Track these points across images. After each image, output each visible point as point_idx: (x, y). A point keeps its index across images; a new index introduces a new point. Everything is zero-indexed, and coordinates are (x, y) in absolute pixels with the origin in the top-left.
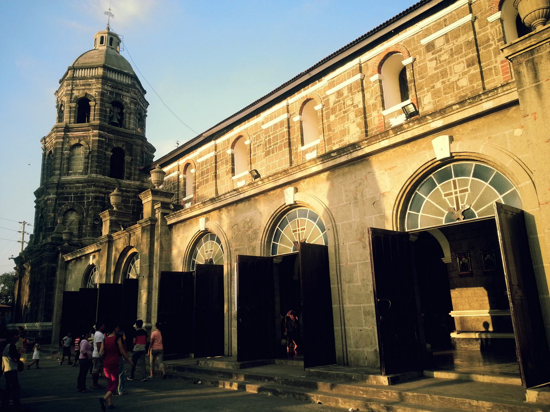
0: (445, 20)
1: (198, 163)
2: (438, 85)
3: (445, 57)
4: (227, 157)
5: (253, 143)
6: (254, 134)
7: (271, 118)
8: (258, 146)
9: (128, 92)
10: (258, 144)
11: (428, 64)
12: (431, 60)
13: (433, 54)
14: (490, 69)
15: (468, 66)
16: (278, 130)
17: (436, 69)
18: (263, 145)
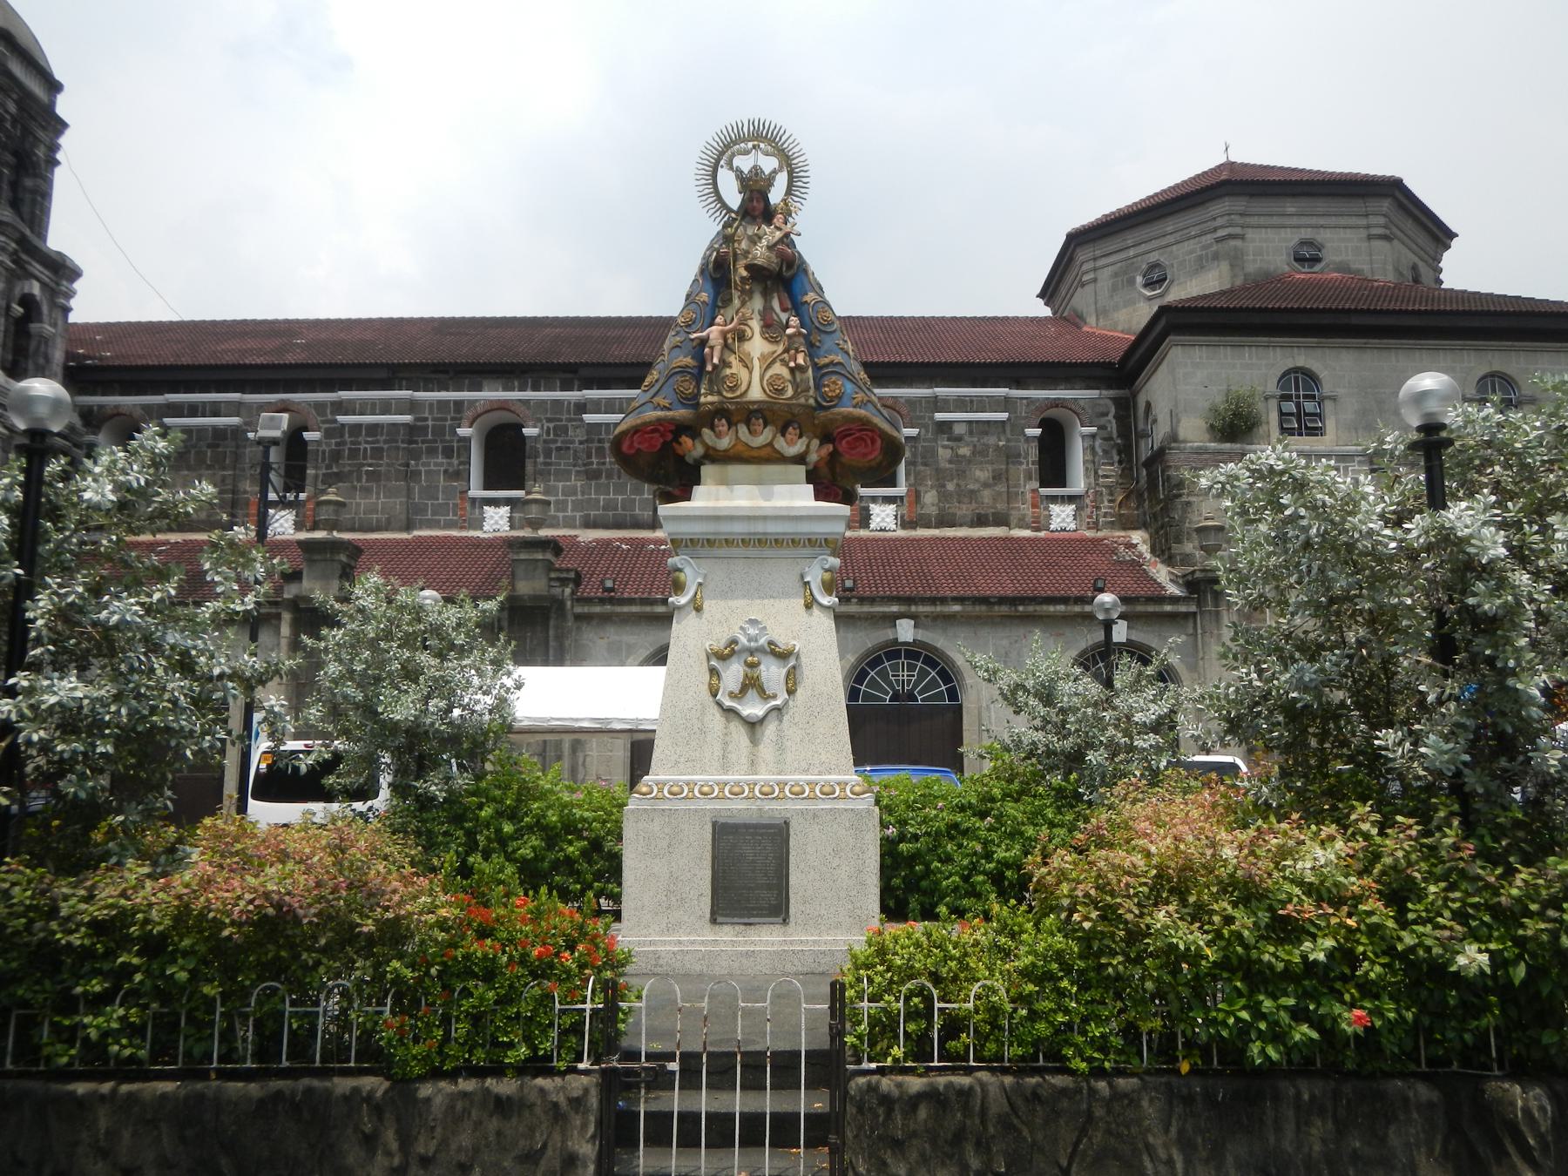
0: (972, 402)
1: (335, 421)
2: (950, 487)
3: (965, 451)
4: (452, 441)
6: (549, 420)
8: (559, 449)
9: (44, 128)
11: (940, 450)
12: (945, 447)
13: (949, 440)
14: (1017, 494)
15: (994, 478)
17: (950, 462)
18: (575, 451)
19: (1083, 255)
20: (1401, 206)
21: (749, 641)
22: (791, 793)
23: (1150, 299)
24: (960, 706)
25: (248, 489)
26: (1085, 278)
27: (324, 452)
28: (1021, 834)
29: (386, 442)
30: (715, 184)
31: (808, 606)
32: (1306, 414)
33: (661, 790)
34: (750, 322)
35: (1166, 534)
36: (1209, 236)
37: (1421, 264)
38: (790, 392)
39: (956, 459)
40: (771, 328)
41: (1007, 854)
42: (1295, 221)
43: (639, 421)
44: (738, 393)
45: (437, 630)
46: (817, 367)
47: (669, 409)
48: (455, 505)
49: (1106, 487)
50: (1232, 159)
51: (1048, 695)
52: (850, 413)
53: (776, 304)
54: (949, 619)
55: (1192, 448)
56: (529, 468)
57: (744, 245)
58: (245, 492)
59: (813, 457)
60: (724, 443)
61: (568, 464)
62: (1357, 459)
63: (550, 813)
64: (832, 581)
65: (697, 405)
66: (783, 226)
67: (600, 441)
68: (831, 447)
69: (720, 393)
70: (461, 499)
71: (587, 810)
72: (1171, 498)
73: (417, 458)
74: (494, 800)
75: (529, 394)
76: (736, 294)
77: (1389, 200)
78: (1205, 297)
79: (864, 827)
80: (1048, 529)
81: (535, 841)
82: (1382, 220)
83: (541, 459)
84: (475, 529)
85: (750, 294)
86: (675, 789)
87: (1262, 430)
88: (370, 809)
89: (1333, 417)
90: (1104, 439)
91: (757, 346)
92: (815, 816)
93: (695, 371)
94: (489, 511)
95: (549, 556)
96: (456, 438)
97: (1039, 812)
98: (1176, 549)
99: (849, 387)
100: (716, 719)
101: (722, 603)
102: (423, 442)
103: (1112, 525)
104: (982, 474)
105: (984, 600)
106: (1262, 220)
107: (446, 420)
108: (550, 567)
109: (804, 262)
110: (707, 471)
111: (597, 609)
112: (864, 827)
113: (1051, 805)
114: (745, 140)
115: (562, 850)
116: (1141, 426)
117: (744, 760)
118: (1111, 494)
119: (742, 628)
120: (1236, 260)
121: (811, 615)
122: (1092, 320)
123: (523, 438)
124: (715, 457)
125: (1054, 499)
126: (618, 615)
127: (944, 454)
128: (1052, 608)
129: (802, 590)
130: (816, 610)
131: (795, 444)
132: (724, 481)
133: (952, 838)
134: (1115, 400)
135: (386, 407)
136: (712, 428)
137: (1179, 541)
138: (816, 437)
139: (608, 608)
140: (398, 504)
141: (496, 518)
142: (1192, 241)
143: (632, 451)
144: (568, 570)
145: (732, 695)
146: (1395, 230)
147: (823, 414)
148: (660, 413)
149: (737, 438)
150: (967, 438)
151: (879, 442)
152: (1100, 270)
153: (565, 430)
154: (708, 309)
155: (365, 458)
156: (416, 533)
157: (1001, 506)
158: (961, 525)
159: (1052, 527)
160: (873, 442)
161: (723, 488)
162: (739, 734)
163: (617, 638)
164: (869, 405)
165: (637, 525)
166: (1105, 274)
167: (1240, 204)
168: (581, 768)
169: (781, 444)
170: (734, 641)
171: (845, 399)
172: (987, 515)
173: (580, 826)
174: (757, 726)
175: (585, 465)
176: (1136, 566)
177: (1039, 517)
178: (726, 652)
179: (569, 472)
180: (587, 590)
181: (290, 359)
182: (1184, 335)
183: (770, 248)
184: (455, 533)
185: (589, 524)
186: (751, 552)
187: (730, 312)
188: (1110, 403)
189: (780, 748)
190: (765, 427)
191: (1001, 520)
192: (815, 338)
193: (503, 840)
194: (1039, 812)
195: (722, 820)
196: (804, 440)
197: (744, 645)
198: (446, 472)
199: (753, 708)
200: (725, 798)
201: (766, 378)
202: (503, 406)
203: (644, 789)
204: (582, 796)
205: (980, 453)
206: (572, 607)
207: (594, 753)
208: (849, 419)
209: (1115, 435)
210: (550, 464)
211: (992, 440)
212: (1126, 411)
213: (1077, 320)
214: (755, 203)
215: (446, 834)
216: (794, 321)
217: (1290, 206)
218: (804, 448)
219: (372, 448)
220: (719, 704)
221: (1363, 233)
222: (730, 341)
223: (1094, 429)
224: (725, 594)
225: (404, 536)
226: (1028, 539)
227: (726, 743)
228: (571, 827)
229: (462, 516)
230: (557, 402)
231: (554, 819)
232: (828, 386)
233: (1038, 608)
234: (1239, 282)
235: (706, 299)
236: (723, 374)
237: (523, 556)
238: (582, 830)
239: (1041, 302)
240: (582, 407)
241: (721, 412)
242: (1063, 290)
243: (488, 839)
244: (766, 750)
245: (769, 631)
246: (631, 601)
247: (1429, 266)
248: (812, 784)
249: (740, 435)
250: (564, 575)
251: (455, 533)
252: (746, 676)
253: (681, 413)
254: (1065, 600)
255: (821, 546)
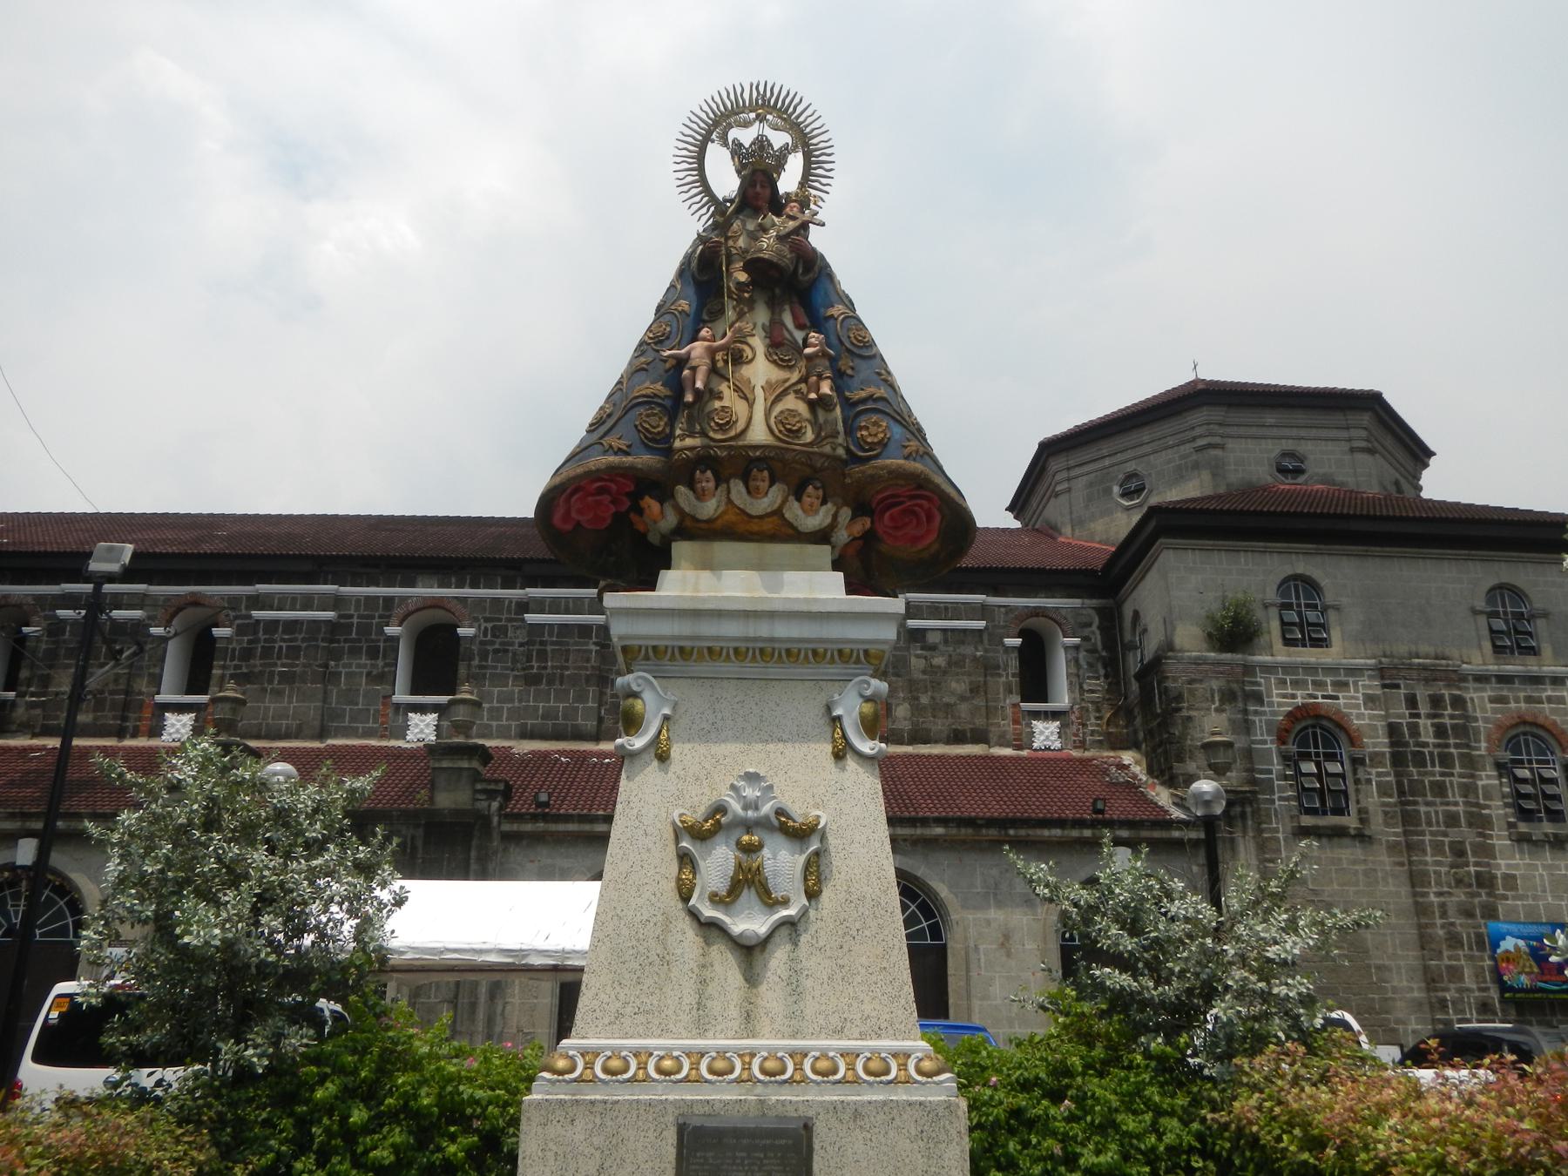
1: (250, 617)
2: (924, 700)
3: (939, 661)
5: (482, 638)
6: (487, 620)
7: (555, 606)
8: (496, 651)
10: (497, 646)
11: (913, 660)
12: (918, 656)
13: (922, 649)
15: (971, 691)
16: (571, 641)
17: (924, 672)
18: (514, 654)
19: (1055, 464)
20: (1382, 422)
21: (746, 808)
22: (815, 1072)
23: (1128, 509)
24: (944, 947)
25: (144, 689)
26: (1058, 488)
27: (234, 650)
28: (1115, 1126)
29: (303, 640)
30: (701, 169)
31: (839, 756)
32: (1309, 624)
33: (589, 1066)
34: (751, 340)
35: (1166, 752)
36: (1188, 445)
37: (1402, 481)
38: (809, 436)
39: (930, 670)
40: (779, 348)
41: (1102, 1159)
42: (1275, 432)
43: (579, 470)
44: (732, 433)
45: (282, 817)
46: (848, 404)
47: (627, 454)
48: (377, 711)
49: (1092, 702)
50: (1201, 377)
51: (1134, 921)
52: (900, 466)
53: (788, 319)
54: (930, 843)
55: (1189, 658)
56: (462, 671)
57: (741, 243)
58: (140, 693)
59: (842, 536)
60: (709, 508)
61: (507, 668)
62: (1366, 673)
63: (424, 1091)
64: (876, 716)
65: (669, 452)
66: (799, 215)
67: (542, 643)
68: (867, 522)
69: (704, 434)
70: (384, 704)
71: (481, 1087)
72: (1170, 712)
73: (338, 658)
74: (341, 1070)
75: (467, 592)
76: (730, 305)
77: (1370, 413)
78: (1194, 500)
79: (943, 1137)
80: (1030, 747)
81: (398, 1136)
82: (1364, 434)
83: (476, 662)
84: (397, 738)
85: (751, 304)
86: (615, 1064)
87: (1263, 640)
88: (159, 1083)
89: (1338, 628)
90: (1087, 651)
91: (760, 371)
92: (857, 1113)
93: (668, 403)
94: (414, 718)
95: (475, 764)
96: (382, 638)
97: (1138, 1091)
98: (1178, 768)
99: (897, 431)
100: (687, 939)
101: (702, 749)
102: (346, 641)
103: (1099, 744)
104: (958, 685)
105: (970, 822)
106: (1242, 431)
107: (373, 617)
108: (476, 777)
109: (828, 266)
110: (680, 549)
111: (528, 827)
112: (943, 1137)
113: (1151, 1084)
114: (743, 109)
115: (439, 1149)
116: (1128, 637)
117: (734, 1012)
118: (1098, 710)
119: (733, 787)
120: (1217, 470)
121: (843, 769)
122: (1067, 530)
123: (458, 638)
124: (692, 529)
125: (1037, 715)
126: (552, 834)
127: (917, 664)
128: (1046, 833)
129: (828, 729)
130: (851, 763)
131: (816, 512)
132: (707, 565)
133: (1012, 1132)
134: (1098, 610)
135: (307, 602)
136: (691, 485)
137: (1181, 760)
138: (848, 505)
139: (541, 826)
140: (312, 709)
141: (422, 725)
142: (1169, 451)
143: (568, 527)
144: (497, 781)
145: (715, 899)
146: (1376, 444)
147: (857, 469)
148: (612, 459)
149: (730, 501)
150: (941, 647)
151: (938, 518)
152: (1075, 480)
153: (504, 630)
154: (689, 321)
155: (279, 658)
156: (330, 742)
157: (980, 722)
158: (936, 742)
159: (1035, 745)
160: (930, 518)
161: (706, 575)
162: (726, 967)
163: (549, 861)
164: (926, 457)
165: (579, 736)
166: (1080, 484)
167: (1217, 414)
168: (499, 1018)
169: (794, 512)
170: (721, 809)
171: (892, 446)
172: (963, 732)
173: (469, 1111)
174: (757, 952)
175: (524, 669)
176: (1132, 787)
177: (1021, 734)
178: (707, 825)
179: (507, 677)
180: (519, 805)
181: (206, 548)
182: (1175, 538)
183: (780, 238)
184: (373, 742)
185: (525, 735)
186: (750, 669)
187: (721, 326)
188: (1092, 613)
189: (795, 991)
190: (771, 486)
191: (980, 737)
192: (845, 364)
193: (350, 1135)
194: (1138, 1091)
195: (696, 1122)
196: (829, 507)
197: (735, 815)
198: (368, 674)
199: (750, 922)
200: (700, 1080)
201: (774, 414)
202: (436, 604)
203: (561, 1064)
204: (475, 1065)
205: (955, 663)
206: (500, 823)
207: (516, 1000)
208: (897, 475)
209: (1100, 646)
210: (485, 667)
211: (968, 650)
212: (1110, 620)
213: (1051, 531)
214: (758, 188)
215: (267, 1123)
216: (814, 337)
217: (1270, 418)
218: (828, 520)
219: (288, 647)
220: (694, 914)
221: (1345, 446)
222: (720, 364)
223: (1077, 640)
224: (708, 735)
225: (316, 744)
226: (1011, 758)
227: (704, 982)
228: (454, 1113)
229: (383, 723)
230: (497, 601)
231: (426, 1102)
232: (867, 428)
233: (1031, 832)
234: (1222, 490)
235: (686, 308)
236: (707, 410)
237: (445, 764)
238: (472, 1117)
239: (1010, 515)
240: (524, 606)
241: (704, 460)
242: (1034, 502)
243: (327, 1131)
244: (771, 994)
245: (777, 792)
246: (567, 818)
247: (1411, 484)
248: (850, 1055)
249: (733, 496)
250: (492, 787)
251: (373, 742)
252: (739, 866)
253: (644, 460)
254: (1061, 823)
255: (858, 661)
